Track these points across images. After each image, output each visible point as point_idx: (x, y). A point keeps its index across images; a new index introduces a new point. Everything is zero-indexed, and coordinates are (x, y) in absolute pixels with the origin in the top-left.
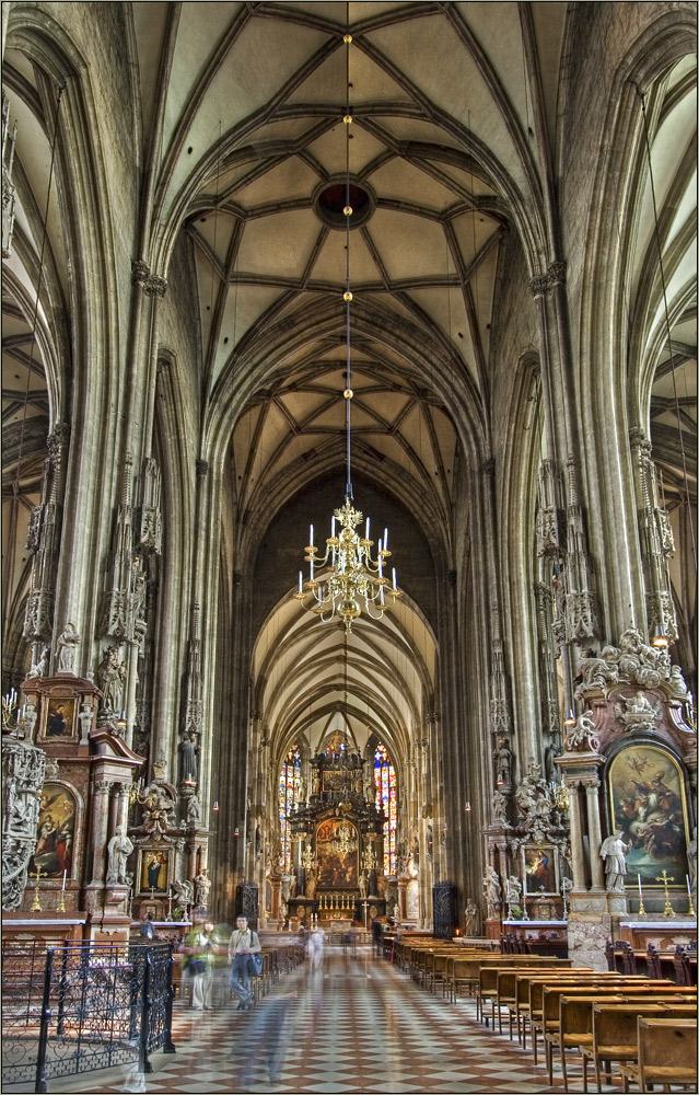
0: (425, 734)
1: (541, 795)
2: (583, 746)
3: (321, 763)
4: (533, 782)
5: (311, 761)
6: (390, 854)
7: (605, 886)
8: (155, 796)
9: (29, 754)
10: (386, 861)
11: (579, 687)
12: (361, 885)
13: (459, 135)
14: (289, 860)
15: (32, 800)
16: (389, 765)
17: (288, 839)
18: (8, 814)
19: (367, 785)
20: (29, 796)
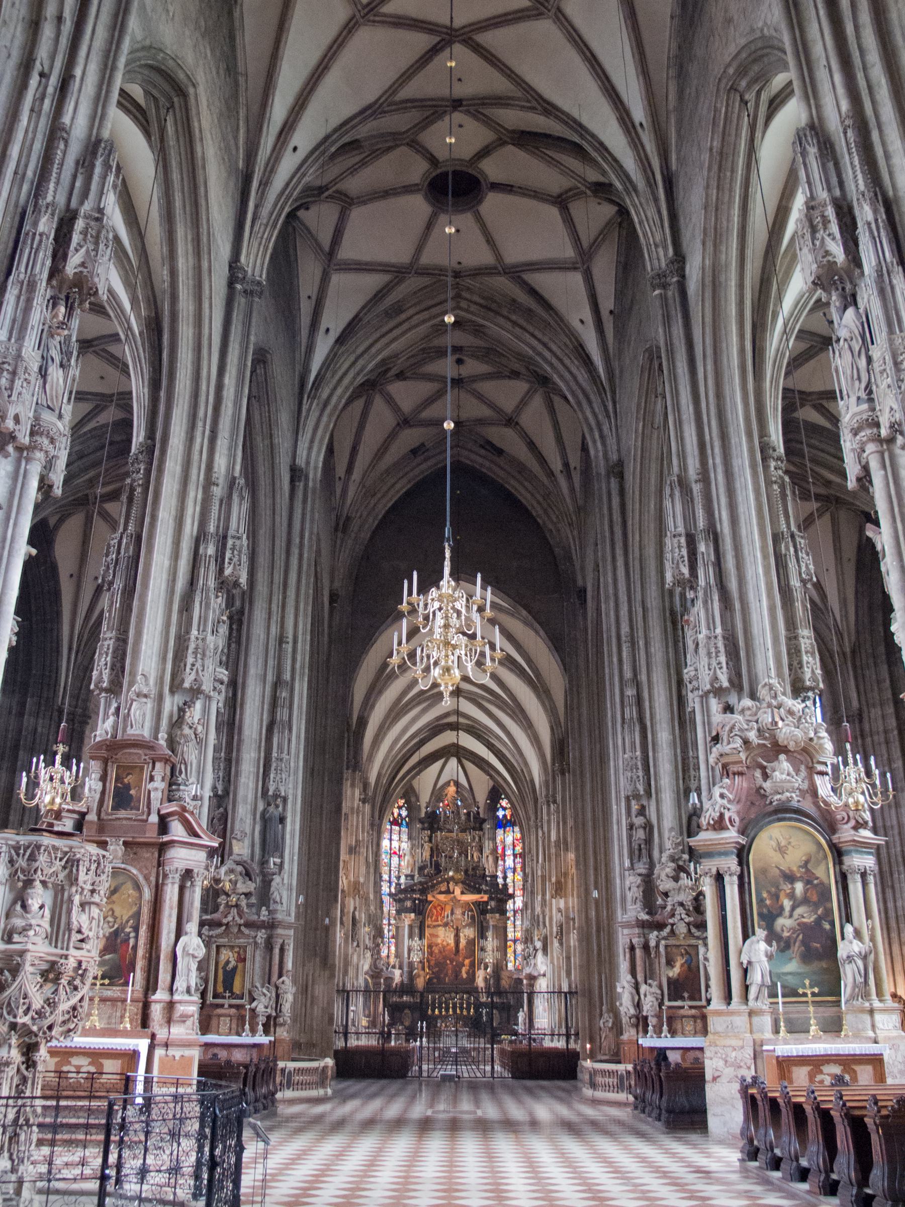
0: (555, 789)
1: (683, 875)
2: (719, 825)
3: (432, 822)
4: (673, 859)
5: (421, 821)
6: (515, 941)
7: (745, 998)
8: (232, 876)
9: (94, 858)
10: (510, 951)
11: (714, 749)
12: (480, 982)
13: (571, 128)
14: (393, 948)
15: (95, 911)
16: (513, 824)
17: (393, 922)
18: (70, 930)
19: (487, 851)
20: (94, 908)
